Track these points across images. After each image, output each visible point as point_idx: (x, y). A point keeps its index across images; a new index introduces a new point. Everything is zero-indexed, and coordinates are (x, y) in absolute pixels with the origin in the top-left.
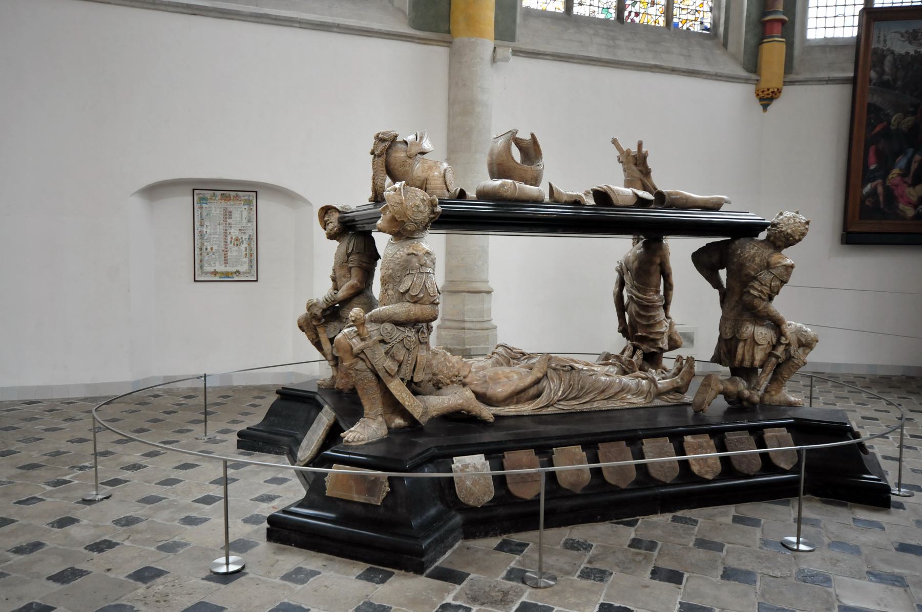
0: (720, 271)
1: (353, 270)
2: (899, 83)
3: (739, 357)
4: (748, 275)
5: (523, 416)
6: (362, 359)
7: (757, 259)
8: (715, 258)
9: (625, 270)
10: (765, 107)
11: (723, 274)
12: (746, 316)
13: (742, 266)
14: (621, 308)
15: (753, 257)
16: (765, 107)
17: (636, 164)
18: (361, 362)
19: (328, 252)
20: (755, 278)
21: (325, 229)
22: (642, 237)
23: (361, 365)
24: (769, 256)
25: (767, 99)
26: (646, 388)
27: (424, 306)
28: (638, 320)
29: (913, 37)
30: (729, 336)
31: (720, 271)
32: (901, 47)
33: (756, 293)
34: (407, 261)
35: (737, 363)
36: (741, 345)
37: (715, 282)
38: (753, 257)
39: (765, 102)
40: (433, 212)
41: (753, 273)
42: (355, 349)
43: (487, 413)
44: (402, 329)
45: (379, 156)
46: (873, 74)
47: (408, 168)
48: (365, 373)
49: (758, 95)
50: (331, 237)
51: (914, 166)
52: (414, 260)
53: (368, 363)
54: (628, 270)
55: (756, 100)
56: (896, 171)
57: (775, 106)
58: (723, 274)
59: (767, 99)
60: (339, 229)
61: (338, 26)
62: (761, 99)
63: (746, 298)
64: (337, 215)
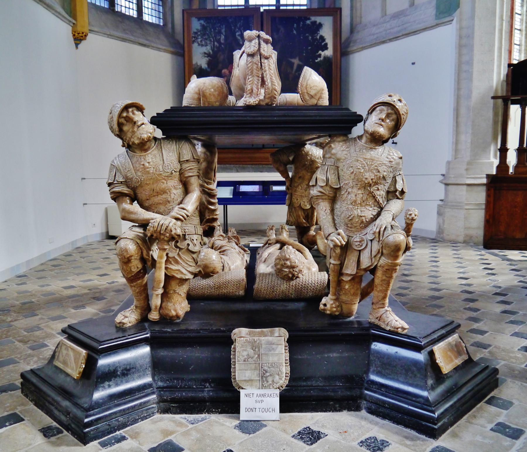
16: (77, 45)
25: (79, 38)
30: (308, 207)
39: (78, 42)
45: (267, 58)
49: (74, 35)
57: (83, 45)
59: (79, 38)
62: (75, 39)
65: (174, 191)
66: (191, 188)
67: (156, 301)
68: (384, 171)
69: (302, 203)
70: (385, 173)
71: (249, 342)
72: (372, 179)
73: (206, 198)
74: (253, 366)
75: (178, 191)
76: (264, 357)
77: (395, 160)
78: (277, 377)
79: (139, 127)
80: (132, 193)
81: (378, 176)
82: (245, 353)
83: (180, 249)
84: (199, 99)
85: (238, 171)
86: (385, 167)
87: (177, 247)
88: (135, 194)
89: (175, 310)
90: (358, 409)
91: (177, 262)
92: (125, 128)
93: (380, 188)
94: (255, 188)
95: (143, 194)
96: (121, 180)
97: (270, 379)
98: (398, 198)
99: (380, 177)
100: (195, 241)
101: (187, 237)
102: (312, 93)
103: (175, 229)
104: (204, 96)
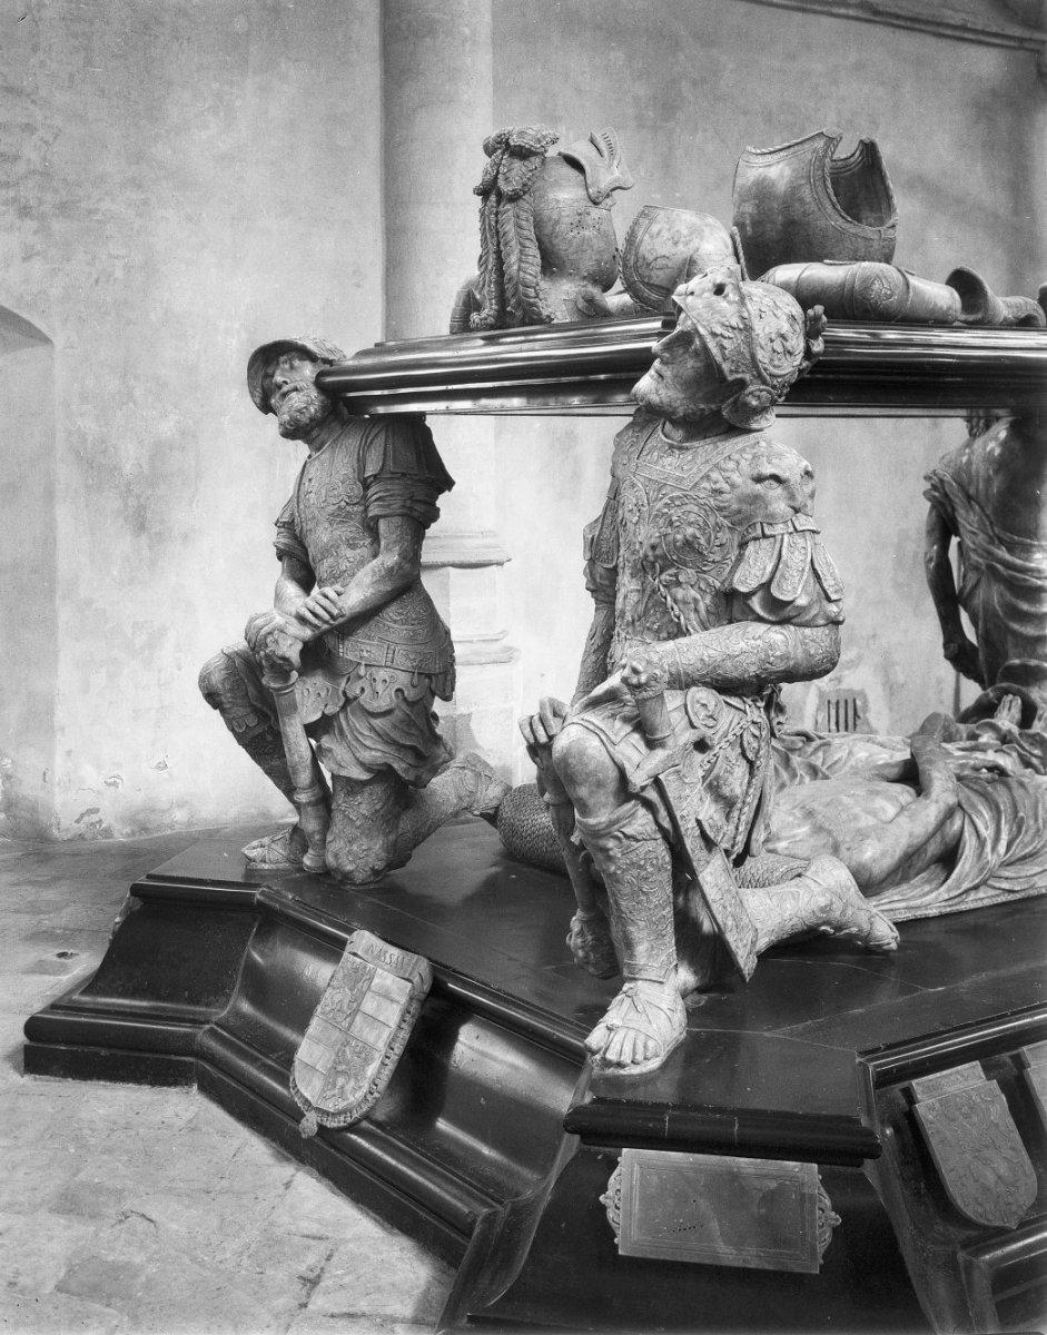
1: (382, 525)
5: (927, 919)
6: (648, 805)
9: (958, 500)
14: (948, 599)
18: (642, 811)
19: (256, 473)
21: (266, 407)
22: (1000, 412)
23: (641, 822)
27: (807, 631)
28: (1016, 626)
40: (808, 354)
42: (638, 779)
43: (880, 922)
44: (735, 701)
48: (650, 845)
50: (293, 431)
52: (774, 492)
53: (663, 813)
54: (969, 497)
60: (324, 408)
64: (308, 371)
65: (349, 553)
68: (690, 524)
70: (690, 530)
72: (653, 547)
73: (1001, 595)
75: (358, 551)
77: (733, 486)
79: (284, 395)
81: (670, 538)
86: (696, 509)
89: (336, 856)
93: (681, 578)
98: (760, 619)
99: (675, 541)
101: (362, 671)
103: (276, 642)
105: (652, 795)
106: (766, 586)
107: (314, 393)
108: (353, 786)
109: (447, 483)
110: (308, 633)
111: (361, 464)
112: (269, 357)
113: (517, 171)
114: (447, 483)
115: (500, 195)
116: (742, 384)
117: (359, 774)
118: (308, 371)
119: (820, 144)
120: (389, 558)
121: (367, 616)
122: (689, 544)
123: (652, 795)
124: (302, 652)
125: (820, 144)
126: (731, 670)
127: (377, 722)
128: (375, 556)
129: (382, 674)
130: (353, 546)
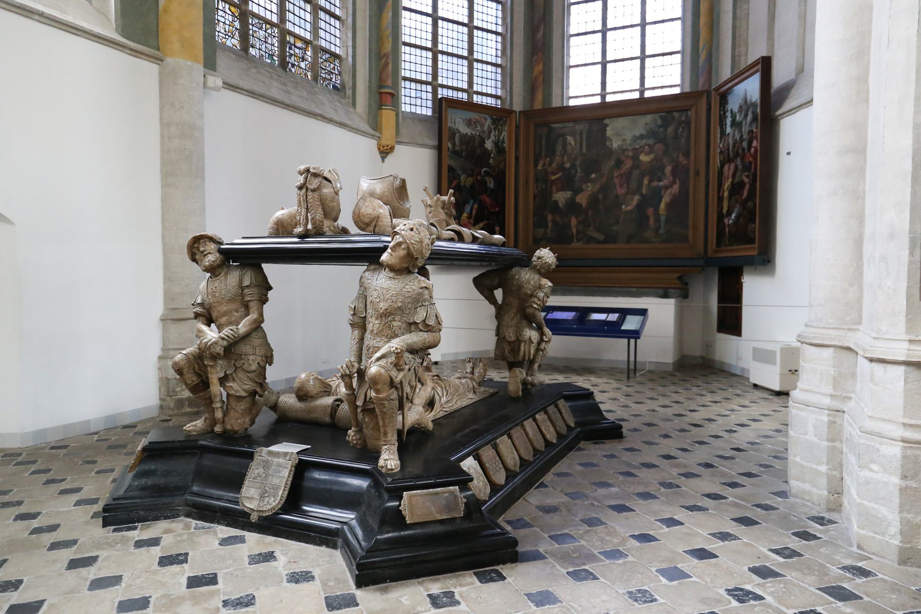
0: (495, 292)
1: (252, 304)
2: (464, 153)
3: (522, 353)
4: (526, 294)
7: (532, 282)
8: (496, 282)
10: (383, 159)
11: (499, 294)
12: (525, 323)
13: (520, 287)
15: (528, 282)
17: (443, 208)
20: (532, 296)
24: (540, 280)
26: (471, 386)
29: (469, 123)
30: (513, 339)
31: (495, 292)
32: (464, 130)
33: (535, 306)
34: (421, 294)
35: (520, 358)
36: (523, 344)
37: (492, 300)
38: (528, 282)
41: (529, 292)
45: (314, 191)
46: (450, 145)
47: (335, 204)
51: (474, 212)
52: (426, 292)
55: (377, 153)
56: (465, 215)
58: (499, 294)
61: (42, 15)
63: (530, 310)
65: (236, 314)
66: (251, 311)
67: (219, 414)
69: (507, 334)
71: (264, 462)
74: (258, 485)
76: (270, 478)
78: (273, 499)
80: (207, 314)
82: (256, 472)
83: (236, 368)
84: (278, 229)
85: (564, 294)
87: (234, 365)
88: (210, 315)
90: (334, 547)
91: (234, 380)
92: (197, 257)
94: (569, 316)
95: (214, 315)
96: (199, 301)
97: (266, 499)
98: (421, 331)
100: (251, 362)
102: (366, 220)
104: (283, 226)
105: (399, 386)
106: (424, 321)
107: (218, 255)
108: (239, 398)
109: (271, 288)
110: (225, 343)
111: (241, 281)
112: (197, 240)
113: (314, 183)
114: (271, 288)
115: (307, 189)
116: (417, 259)
117: (244, 394)
118: (212, 247)
119: (392, 178)
120: (253, 316)
121: (246, 336)
122: (399, 308)
123: (399, 386)
124: (225, 351)
125: (392, 178)
126: (415, 347)
127: (249, 375)
128: (247, 315)
129: (252, 357)
130: (237, 311)
